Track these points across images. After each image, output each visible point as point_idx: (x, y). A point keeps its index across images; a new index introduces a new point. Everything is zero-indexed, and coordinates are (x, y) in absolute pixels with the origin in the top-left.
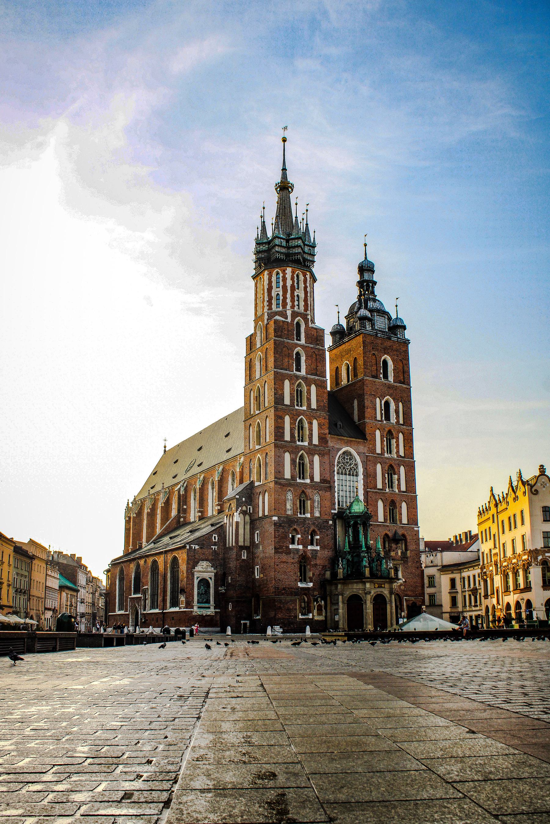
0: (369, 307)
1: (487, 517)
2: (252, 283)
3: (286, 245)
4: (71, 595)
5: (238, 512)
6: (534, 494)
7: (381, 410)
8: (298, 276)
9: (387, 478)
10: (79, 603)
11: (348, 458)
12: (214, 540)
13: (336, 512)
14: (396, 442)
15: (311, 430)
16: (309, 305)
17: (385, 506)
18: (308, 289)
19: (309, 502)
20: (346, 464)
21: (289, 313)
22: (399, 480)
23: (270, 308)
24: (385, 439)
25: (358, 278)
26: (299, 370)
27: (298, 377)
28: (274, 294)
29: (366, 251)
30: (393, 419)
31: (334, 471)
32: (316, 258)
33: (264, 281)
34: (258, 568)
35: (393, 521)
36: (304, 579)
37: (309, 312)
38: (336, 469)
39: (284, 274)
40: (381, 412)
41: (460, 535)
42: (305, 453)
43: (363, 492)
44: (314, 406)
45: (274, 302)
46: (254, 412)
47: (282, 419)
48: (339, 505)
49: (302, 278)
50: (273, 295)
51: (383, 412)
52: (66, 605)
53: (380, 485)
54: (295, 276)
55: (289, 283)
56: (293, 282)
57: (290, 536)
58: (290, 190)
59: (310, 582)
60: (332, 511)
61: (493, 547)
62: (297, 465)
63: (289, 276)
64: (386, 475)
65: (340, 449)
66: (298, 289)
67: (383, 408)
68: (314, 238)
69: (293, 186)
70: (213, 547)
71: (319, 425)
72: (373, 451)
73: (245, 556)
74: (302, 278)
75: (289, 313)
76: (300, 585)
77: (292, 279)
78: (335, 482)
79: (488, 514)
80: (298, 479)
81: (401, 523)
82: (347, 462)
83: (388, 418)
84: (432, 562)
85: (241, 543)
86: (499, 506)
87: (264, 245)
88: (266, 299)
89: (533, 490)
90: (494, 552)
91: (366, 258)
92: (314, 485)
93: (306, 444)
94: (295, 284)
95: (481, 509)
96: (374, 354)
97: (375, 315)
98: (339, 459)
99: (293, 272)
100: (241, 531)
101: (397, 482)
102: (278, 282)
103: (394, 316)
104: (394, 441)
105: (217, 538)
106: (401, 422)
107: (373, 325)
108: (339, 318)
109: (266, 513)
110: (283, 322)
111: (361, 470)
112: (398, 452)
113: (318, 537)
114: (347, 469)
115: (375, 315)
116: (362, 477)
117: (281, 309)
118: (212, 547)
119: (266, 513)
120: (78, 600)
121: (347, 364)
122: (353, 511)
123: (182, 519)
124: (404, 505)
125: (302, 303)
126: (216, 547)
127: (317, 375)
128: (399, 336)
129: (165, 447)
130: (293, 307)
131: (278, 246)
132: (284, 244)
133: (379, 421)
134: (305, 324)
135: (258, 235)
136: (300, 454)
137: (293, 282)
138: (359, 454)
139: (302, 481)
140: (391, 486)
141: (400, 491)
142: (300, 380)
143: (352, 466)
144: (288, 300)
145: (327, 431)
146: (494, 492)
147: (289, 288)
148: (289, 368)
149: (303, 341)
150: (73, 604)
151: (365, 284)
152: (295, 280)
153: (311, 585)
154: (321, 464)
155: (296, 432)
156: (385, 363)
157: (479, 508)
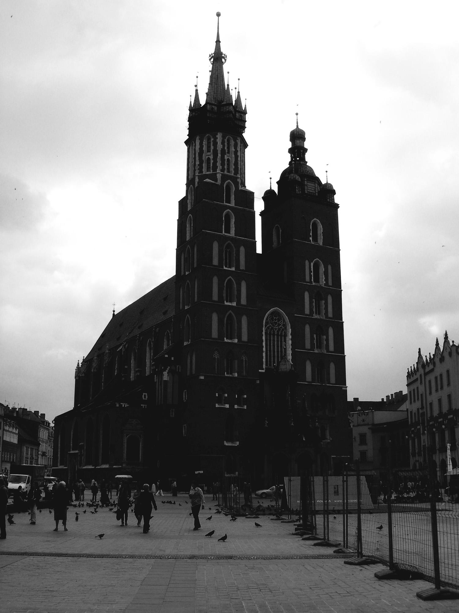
1: (415, 377)
4: (31, 448)
5: (167, 371)
7: (310, 272)
10: (40, 456)
13: (264, 371)
15: (239, 291)
16: (239, 169)
18: (239, 154)
19: (236, 362)
21: (219, 176)
22: (327, 340)
23: (201, 171)
25: (290, 145)
26: (228, 230)
28: (204, 158)
29: (297, 120)
30: (322, 281)
32: (247, 124)
33: (195, 146)
37: (239, 176)
38: (264, 329)
39: (216, 138)
41: (392, 395)
42: (232, 313)
46: (185, 273)
48: (266, 365)
49: (232, 143)
50: (204, 158)
51: (312, 274)
52: (26, 458)
54: (226, 140)
55: (220, 146)
56: (224, 146)
58: (223, 60)
60: (260, 371)
62: (225, 325)
63: (219, 141)
64: (315, 336)
66: (229, 153)
67: (312, 270)
69: (226, 57)
74: (232, 143)
75: (219, 176)
77: (223, 143)
79: (416, 374)
80: (225, 338)
82: (276, 323)
83: (317, 279)
88: (197, 163)
91: (297, 126)
94: (226, 148)
95: (410, 370)
97: (305, 179)
98: (267, 319)
99: (224, 137)
101: (325, 342)
102: (209, 147)
105: (147, 397)
106: (330, 283)
107: (303, 190)
108: (271, 183)
109: (194, 372)
114: (276, 329)
116: (290, 337)
118: (142, 405)
119: (194, 372)
120: (40, 453)
124: (332, 366)
128: (328, 200)
129: (114, 311)
130: (223, 170)
136: (228, 314)
137: (224, 146)
144: (219, 164)
147: (219, 152)
149: (232, 204)
150: (34, 456)
151: (296, 151)
152: (226, 144)
155: (225, 292)
156: (315, 225)
157: (408, 369)
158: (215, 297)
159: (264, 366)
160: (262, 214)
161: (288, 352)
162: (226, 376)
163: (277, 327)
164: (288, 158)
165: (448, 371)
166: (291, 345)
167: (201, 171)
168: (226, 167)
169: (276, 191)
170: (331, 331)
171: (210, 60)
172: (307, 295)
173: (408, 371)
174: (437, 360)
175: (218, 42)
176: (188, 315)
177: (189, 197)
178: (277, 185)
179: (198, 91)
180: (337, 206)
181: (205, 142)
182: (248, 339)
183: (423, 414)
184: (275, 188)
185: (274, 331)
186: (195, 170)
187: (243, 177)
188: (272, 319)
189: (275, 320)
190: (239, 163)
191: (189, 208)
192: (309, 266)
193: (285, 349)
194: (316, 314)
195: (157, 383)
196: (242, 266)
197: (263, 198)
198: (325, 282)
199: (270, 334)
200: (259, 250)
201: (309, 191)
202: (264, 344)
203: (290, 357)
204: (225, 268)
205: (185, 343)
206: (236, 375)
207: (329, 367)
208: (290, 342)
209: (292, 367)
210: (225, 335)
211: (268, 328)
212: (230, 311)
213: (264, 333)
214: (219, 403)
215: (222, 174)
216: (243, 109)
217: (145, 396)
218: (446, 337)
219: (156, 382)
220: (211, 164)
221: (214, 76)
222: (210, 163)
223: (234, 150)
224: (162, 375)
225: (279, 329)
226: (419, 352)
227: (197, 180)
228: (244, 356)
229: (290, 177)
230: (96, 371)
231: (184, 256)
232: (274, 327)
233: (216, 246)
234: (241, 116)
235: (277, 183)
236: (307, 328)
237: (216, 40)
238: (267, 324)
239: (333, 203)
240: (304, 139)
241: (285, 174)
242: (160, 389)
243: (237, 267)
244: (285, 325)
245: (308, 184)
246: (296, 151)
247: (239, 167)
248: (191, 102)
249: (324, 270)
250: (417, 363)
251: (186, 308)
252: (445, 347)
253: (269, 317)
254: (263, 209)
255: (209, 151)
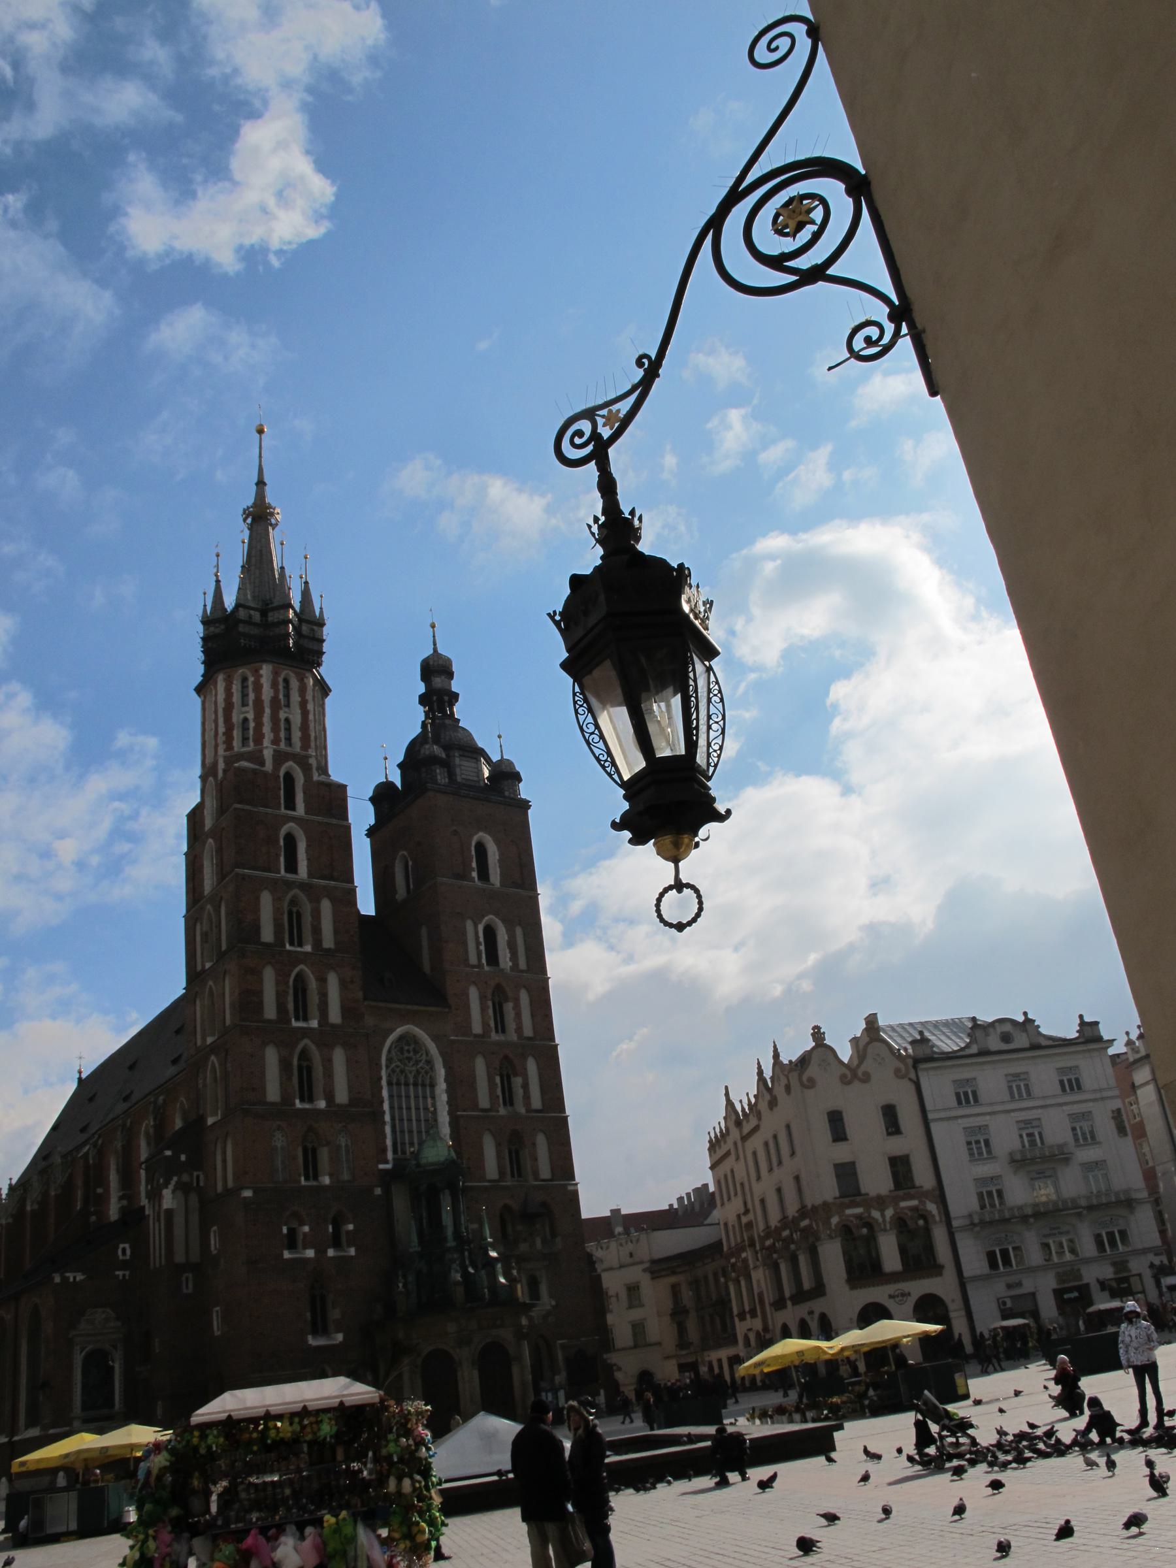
0: (442, 740)
2: (197, 701)
3: (261, 621)
5: (171, 1187)
6: (808, 1087)
7: (478, 944)
8: (286, 681)
9: (499, 1085)
11: (411, 1048)
12: (121, 1257)
13: (389, 1166)
14: (513, 1009)
15: (324, 995)
17: (498, 1145)
18: (310, 707)
20: (406, 1061)
21: (268, 754)
22: (525, 1086)
23: (229, 747)
24: (490, 1003)
25: (421, 688)
26: (292, 867)
27: (289, 885)
28: (236, 718)
29: (434, 636)
31: (380, 1078)
32: (326, 647)
33: (216, 695)
34: (217, 1312)
35: (520, 1175)
36: (320, 1326)
37: (312, 752)
38: (384, 1073)
39: (258, 677)
40: (478, 948)
41: (688, 1195)
42: (313, 1047)
43: (447, 1119)
44: (328, 942)
45: (236, 733)
46: (203, 966)
47: (257, 973)
48: (395, 1151)
51: (482, 948)
53: (484, 1101)
54: (280, 680)
55: (267, 693)
56: (276, 691)
57: (285, 1230)
59: (338, 1332)
60: (381, 1166)
61: (742, 1210)
63: (266, 682)
64: (498, 1079)
65: (392, 1030)
66: (288, 705)
67: (482, 940)
68: (321, 608)
70: (120, 1273)
71: (343, 984)
72: (466, 1028)
73: (191, 1285)
74: (294, 684)
75: (268, 754)
76: (312, 1341)
77: (274, 685)
78: (382, 1102)
79: (725, 1142)
80: (297, 1101)
81: (536, 1178)
82: (409, 1059)
83: (493, 958)
84: (631, 1255)
85: (179, 1258)
86: (744, 1123)
87: (217, 625)
88: (221, 729)
89: (805, 1078)
90: (744, 1220)
91: (435, 650)
92: (335, 1112)
93: (314, 1024)
94: (281, 696)
95: (713, 1135)
96: (455, 831)
97: (457, 754)
98: (389, 1051)
99: (276, 674)
100: (179, 1231)
101: (521, 1092)
102: (244, 695)
103: (495, 758)
104: (509, 1007)
105: (128, 1252)
106: (523, 964)
107: (451, 775)
109: (230, 1184)
110: (254, 772)
111: (441, 1072)
112: (519, 1029)
113: (351, 1227)
115: (457, 754)
117: (251, 746)
118: (117, 1273)
119: (230, 1184)
121: (405, 856)
122: (423, 1161)
123: (93, 1218)
124: (541, 1141)
125: (296, 735)
126: (127, 1273)
127: (332, 878)
128: (507, 794)
129: (80, 1072)
130: (276, 741)
131: (244, 622)
132: (257, 616)
133: (474, 967)
134: (305, 776)
135: (205, 606)
137: (276, 691)
138: (435, 1038)
139: (307, 1106)
140: (509, 1100)
141: (529, 1110)
142: (296, 891)
143: (421, 1065)
144: (267, 729)
145: (360, 995)
146: (732, 1097)
148: (271, 867)
152: (281, 687)
153: (340, 1337)
154: (350, 1063)
155: (291, 999)
156: (481, 849)
158: (270, 1012)
159: (390, 1155)
160: (371, 833)
161: (440, 1119)
162: (304, 1186)
163: (414, 1065)
164: (419, 714)
165: (788, 1127)
166: (448, 1103)
167: (229, 747)
168: (282, 735)
169: (399, 784)
170: (532, 1066)
171: (245, 520)
172: (473, 994)
173: (710, 1137)
174: (763, 1106)
175: (261, 483)
176: (213, 1058)
177: (208, 804)
178: (399, 772)
179: (221, 583)
180: (525, 805)
181: (236, 688)
182: (350, 1100)
183: (749, 1225)
184: (396, 778)
185: (406, 1077)
186: (216, 746)
187: (321, 755)
188: (401, 1051)
189: (408, 1051)
190: (312, 725)
191: (208, 823)
192: (474, 933)
193: (435, 1112)
194: (497, 1032)
195: (151, 1217)
196: (328, 942)
197: (372, 799)
198: (510, 964)
199: (398, 1084)
200: (367, 905)
201: (463, 776)
202: (386, 1106)
203: (445, 1130)
204: (288, 947)
205: (210, 1121)
206: (326, 1180)
207: (534, 1144)
208: (444, 1097)
209: (449, 1150)
210: (297, 1095)
211: (393, 1071)
212: (306, 1041)
213: (384, 1082)
214: (292, 1246)
215: (275, 751)
216: (317, 614)
217: (124, 1250)
218: (776, 1055)
219: (149, 1215)
220: (251, 732)
221: (253, 552)
222: (248, 729)
223: (299, 699)
224: (160, 1197)
225: (418, 1072)
226: (727, 1094)
227: (221, 765)
228: (343, 1137)
229: (422, 751)
230: (36, 1207)
231: (201, 929)
232: (407, 1068)
233: (266, 900)
234: (313, 630)
235: (400, 766)
236: (480, 1066)
237: (256, 480)
238: (391, 1063)
239: (512, 799)
240: (450, 675)
241: (413, 748)
242: (157, 1232)
243: (317, 943)
244: (429, 1062)
245: (465, 763)
246: (435, 698)
247: (313, 735)
248: (205, 606)
249: (506, 938)
250: (725, 1118)
251: (209, 1040)
252: (776, 1077)
253: (393, 1046)
254: (372, 821)
255: (245, 704)
